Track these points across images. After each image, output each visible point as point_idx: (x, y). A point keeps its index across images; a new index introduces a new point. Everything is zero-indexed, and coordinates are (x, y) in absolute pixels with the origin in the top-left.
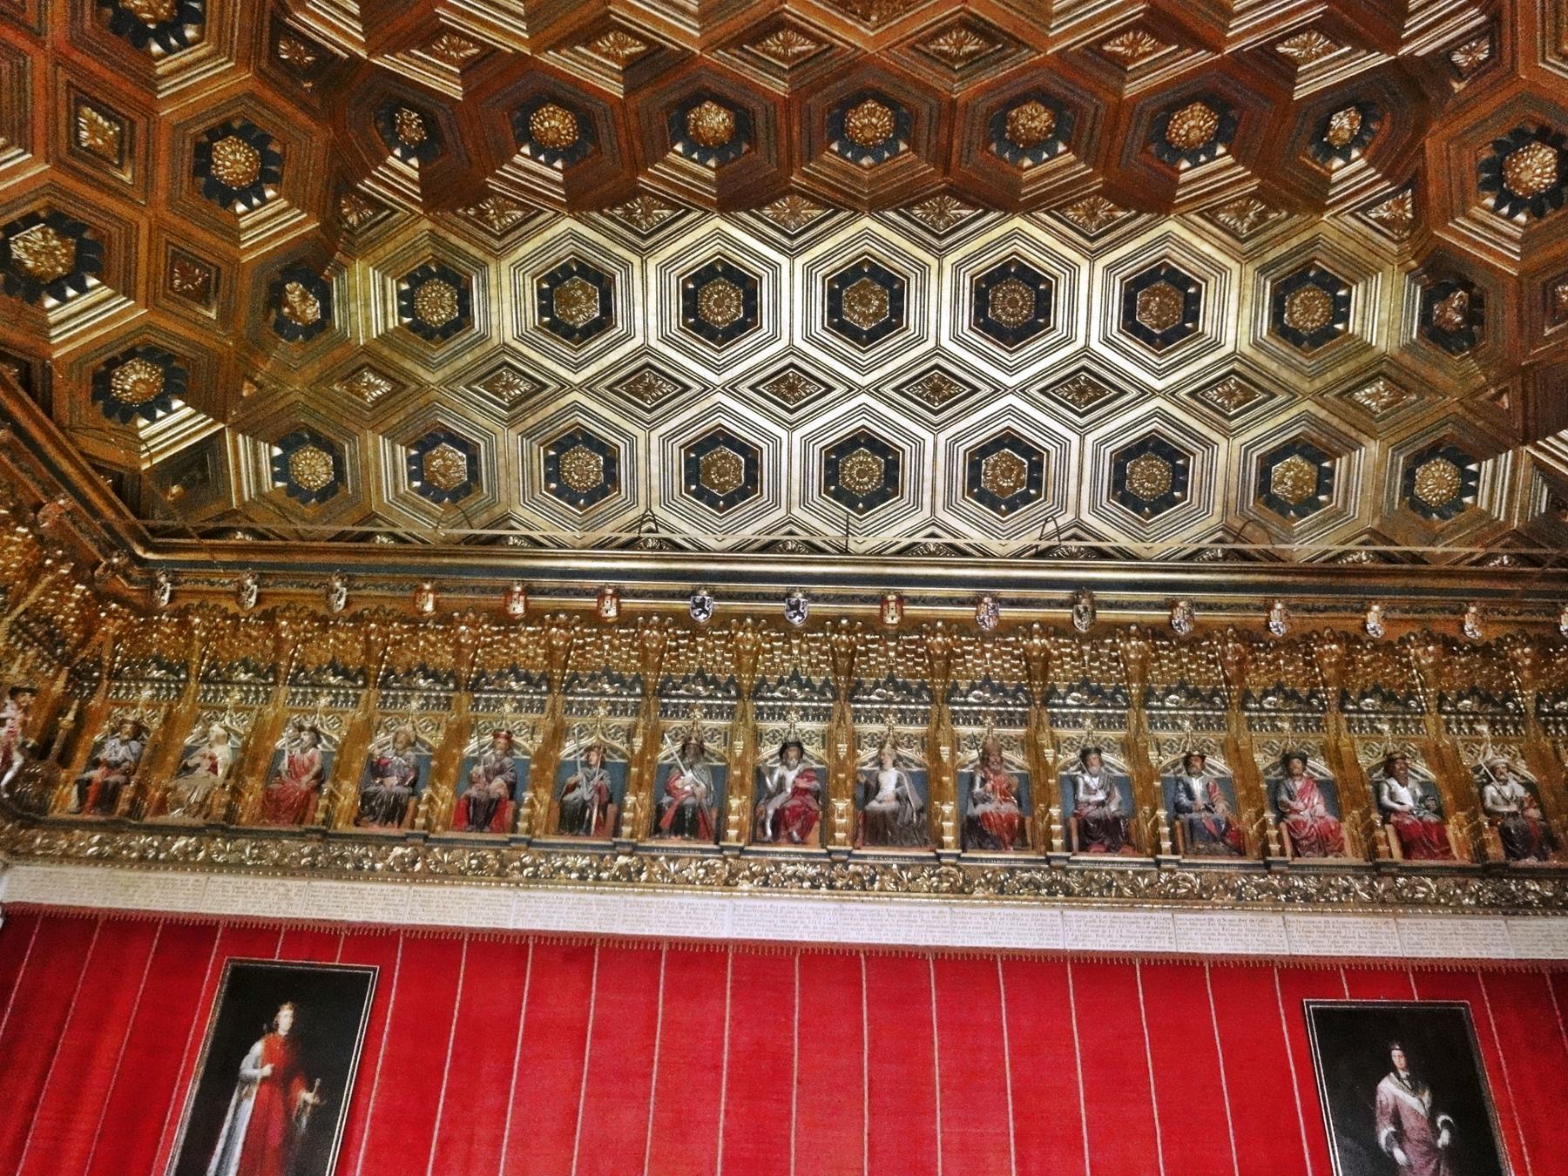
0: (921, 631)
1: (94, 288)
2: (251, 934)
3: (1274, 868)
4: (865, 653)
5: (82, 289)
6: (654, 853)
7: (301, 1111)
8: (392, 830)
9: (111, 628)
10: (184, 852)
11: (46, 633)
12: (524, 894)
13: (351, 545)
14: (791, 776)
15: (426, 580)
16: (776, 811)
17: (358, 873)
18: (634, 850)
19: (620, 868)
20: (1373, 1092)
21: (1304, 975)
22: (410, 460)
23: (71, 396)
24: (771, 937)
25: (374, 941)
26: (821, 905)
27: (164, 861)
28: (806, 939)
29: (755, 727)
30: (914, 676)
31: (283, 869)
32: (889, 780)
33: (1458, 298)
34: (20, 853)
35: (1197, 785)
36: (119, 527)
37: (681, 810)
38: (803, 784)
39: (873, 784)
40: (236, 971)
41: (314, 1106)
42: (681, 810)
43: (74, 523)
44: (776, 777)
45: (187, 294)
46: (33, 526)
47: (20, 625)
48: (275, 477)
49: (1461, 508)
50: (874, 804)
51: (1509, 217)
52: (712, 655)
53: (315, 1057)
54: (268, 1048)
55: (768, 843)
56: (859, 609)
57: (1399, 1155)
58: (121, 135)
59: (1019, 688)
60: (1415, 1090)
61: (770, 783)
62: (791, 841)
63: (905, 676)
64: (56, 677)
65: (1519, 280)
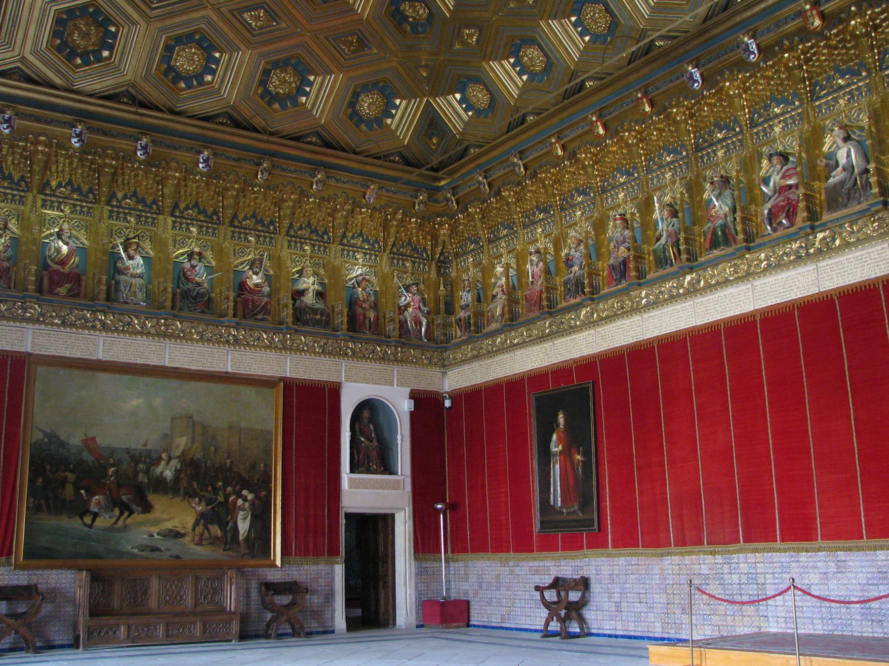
0: (841, 21)
1: (314, 80)
2: (537, 378)
4: (810, 59)
5: (311, 84)
7: (578, 465)
8: (578, 300)
9: (444, 231)
10: (502, 343)
11: (412, 250)
12: (645, 316)
13: (519, 129)
15: (549, 137)
16: (770, 210)
17: (572, 330)
18: (691, 270)
19: (688, 283)
22: (513, 66)
23: (344, 133)
25: (586, 367)
27: (496, 351)
28: (799, 296)
29: (758, 151)
30: (851, 60)
31: (543, 338)
34: (444, 366)
36: (413, 178)
39: (832, 162)
40: (537, 399)
41: (582, 461)
43: (388, 191)
44: (771, 184)
45: (353, 52)
46: (367, 206)
47: (394, 254)
48: (466, 110)
50: (831, 180)
53: (577, 438)
54: (558, 436)
56: (791, 26)
58: (266, 11)
64: (430, 268)
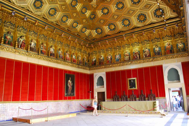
3: (28, 52)
6: (5, 47)
14: (22, 40)
20: (68, 81)
21: (66, 71)
24: (20, 60)
26: (26, 57)
32: (33, 43)
33: (94, 16)
35: (60, 52)
37: (9, 41)
38: (24, 42)
42: (9, 41)
49: (84, 32)
51: (102, 13)
52: (13, 20)
55: (19, 48)
57: (69, 86)
59: (46, 37)
60: (71, 81)
61: (19, 40)
62: (22, 48)
63: (35, 31)
65: (99, 18)
